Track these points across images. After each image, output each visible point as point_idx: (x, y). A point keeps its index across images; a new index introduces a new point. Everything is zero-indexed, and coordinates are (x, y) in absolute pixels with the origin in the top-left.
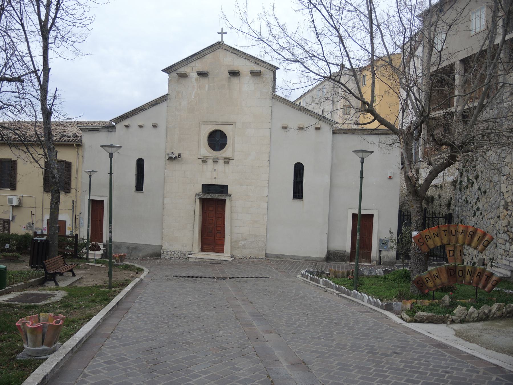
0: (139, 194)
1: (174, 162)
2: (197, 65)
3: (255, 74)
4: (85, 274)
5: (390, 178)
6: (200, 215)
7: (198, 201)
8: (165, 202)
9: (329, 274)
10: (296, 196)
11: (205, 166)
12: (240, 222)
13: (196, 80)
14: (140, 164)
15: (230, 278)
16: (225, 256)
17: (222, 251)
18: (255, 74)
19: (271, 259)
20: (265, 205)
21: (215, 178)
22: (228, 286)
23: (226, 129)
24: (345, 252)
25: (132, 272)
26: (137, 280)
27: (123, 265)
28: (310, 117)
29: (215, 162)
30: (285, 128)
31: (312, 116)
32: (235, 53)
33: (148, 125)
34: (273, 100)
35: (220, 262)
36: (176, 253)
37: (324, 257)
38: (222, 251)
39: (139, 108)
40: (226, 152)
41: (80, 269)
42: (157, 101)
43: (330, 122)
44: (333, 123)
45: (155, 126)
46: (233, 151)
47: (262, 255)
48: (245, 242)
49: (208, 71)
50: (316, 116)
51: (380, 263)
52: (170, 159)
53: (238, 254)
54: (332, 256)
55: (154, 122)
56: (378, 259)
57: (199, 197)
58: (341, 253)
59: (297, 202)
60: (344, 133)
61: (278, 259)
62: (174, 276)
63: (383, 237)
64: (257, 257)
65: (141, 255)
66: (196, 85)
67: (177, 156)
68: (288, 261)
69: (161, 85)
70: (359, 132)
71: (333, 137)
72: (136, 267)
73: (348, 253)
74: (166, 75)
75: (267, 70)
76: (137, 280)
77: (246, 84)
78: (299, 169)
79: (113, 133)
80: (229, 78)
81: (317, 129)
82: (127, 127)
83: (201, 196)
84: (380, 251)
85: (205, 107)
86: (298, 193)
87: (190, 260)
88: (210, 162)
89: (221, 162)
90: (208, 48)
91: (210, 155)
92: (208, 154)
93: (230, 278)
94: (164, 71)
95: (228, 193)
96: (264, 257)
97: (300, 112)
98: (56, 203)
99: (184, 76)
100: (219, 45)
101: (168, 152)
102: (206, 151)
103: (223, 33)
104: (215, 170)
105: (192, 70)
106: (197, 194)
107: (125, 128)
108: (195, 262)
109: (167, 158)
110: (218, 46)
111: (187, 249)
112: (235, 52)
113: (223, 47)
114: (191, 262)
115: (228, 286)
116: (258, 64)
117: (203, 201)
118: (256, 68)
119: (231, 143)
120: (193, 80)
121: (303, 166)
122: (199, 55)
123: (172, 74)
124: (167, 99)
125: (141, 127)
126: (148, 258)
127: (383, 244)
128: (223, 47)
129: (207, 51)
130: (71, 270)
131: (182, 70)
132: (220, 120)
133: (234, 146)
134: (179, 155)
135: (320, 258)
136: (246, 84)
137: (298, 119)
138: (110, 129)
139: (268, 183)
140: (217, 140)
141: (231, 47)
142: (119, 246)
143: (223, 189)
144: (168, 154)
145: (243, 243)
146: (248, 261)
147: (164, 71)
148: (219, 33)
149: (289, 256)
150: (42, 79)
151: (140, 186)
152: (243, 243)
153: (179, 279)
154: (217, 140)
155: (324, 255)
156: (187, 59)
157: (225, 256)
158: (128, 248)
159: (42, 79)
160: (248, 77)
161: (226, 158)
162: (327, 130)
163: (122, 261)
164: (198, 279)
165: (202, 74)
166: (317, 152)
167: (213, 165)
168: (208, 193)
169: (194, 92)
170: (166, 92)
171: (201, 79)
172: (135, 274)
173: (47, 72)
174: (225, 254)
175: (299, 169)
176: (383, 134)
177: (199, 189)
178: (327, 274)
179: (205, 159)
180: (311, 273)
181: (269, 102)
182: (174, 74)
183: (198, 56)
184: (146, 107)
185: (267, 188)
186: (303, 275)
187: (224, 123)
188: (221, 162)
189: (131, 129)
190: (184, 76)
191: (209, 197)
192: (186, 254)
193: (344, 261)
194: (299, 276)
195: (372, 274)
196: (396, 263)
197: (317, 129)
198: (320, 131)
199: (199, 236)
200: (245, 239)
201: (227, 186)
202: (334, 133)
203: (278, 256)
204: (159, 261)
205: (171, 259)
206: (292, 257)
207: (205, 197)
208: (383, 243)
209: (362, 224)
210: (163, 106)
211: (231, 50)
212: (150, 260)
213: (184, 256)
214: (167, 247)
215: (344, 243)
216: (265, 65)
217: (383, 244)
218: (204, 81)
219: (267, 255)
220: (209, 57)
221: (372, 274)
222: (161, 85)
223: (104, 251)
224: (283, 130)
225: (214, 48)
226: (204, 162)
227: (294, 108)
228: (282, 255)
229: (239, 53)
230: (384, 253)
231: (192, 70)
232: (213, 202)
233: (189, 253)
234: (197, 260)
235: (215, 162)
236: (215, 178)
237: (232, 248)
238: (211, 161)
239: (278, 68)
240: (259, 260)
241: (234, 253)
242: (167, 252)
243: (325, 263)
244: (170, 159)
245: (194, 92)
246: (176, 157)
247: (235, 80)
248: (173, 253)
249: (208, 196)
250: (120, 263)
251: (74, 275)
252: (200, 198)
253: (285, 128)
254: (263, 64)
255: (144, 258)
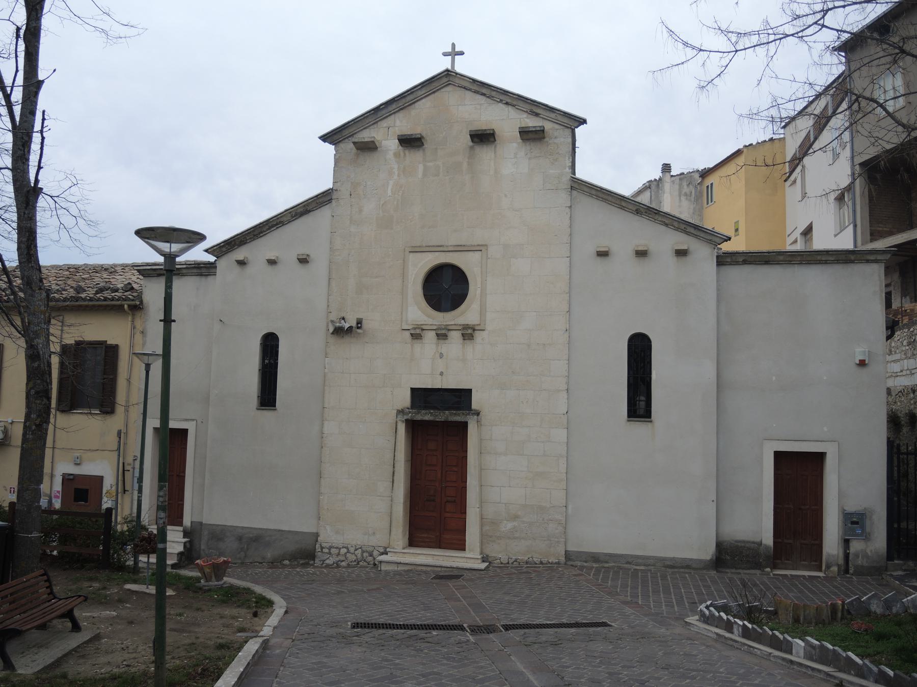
0: (267, 414)
1: (347, 339)
2: (398, 123)
3: (531, 136)
4: (112, 621)
5: (862, 363)
6: (406, 461)
7: (402, 428)
8: (326, 430)
9: (775, 613)
10: (635, 411)
11: (417, 346)
12: (502, 477)
13: (396, 155)
14: (270, 344)
15: (507, 628)
16: (468, 559)
17: (461, 546)
18: (531, 136)
19: (579, 564)
20: (560, 435)
21: (442, 374)
22: (520, 666)
23: (467, 262)
24: (760, 544)
25: (243, 611)
26: (252, 646)
27: (221, 587)
28: (663, 228)
29: (442, 336)
30: (603, 254)
31: (667, 225)
32: (483, 94)
33: (289, 257)
34: (574, 192)
35: (456, 573)
36: (352, 550)
37: (708, 557)
38: (461, 546)
39: (268, 221)
40: (468, 313)
41: (103, 602)
42: (308, 205)
43: (713, 238)
44: (718, 240)
45: (304, 261)
46: (483, 311)
47: (557, 554)
48: (516, 524)
49: (424, 134)
50: (676, 224)
51: (847, 571)
52: (339, 332)
53: (500, 552)
54: (729, 556)
55: (302, 251)
56: (841, 561)
57: (406, 417)
58: (749, 549)
59: (639, 428)
60: (745, 262)
61: (595, 565)
62: (356, 625)
63: (852, 506)
64: (545, 560)
65: (269, 555)
66: (396, 166)
67: (354, 324)
68: (620, 568)
69: (317, 169)
70: (781, 258)
71: (718, 273)
72: (253, 592)
73: (767, 547)
74: (330, 149)
75: (557, 126)
76: (252, 646)
77: (511, 160)
78: (640, 350)
79: (210, 278)
80: (472, 148)
81: (681, 253)
82: (241, 263)
83: (409, 417)
84: (846, 542)
85: (416, 210)
86: (639, 404)
87: (384, 567)
88: (430, 336)
89: (455, 336)
90: (423, 85)
91: (430, 321)
92: (426, 318)
93: (507, 628)
94: (325, 138)
95: (474, 406)
96: (563, 559)
97: (637, 218)
98: (39, 426)
99: (368, 147)
100: (447, 78)
101: (333, 317)
102: (418, 312)
103: (454, 53)
104: (441, 356)
105: (385, 137)
106: (401, 412)
107: (237, 269)
108: (397, 573)
109: (331, 329)
110: (445, 80)
111: (377, 541)
112: (484, 91)
113: (457, 81)
114: (387, 573)
115: (520, 666)
116: (537, 115)
117: (415, 429)
118: (532, 122)
119: (479, 292)
120: (390, 155)
121: (649, 341)
122: (404, 101)
123: (342, 145)
124: (330, 201)
125: (272, 262)
126: (287, 562)
127: (853, 523)
128: (457, 81)
129: (420, 93)
130: (69, 615)
131: (365, 136)
132: (453, 241)
133: (485, 300)
134: (359, 322)
135: (701, 561)
136: (511, 160)
137: (631, 232)
138: (204, 270)
139: (568, 383)
140: (446, 287)
141: (474, 81)
142: (219, 534)
143: (460, 398)
144: (332, 321)
145: (510, 525)
146: (527, 571)
147: (325, 138)
148: (445, 54)
149: (622, 556)
150: (17, 110)
151: (268, 397)
152: (510, 525)
153: (370, 636)
154: (446, 287)
155: (708, 553)
156: (377, 110)
157: (468, 559)
158: (240, 539)
159: (17, 110)
160: (515, 145)
161: (466, 327)
162: (704, 256)
163: (219, 578)
164: (422, 633)
165: (410, 142)
166: (678, 306)
167: (437, 344)
168: (425, 408)
169: (391, 183)
170: (328, 184)
171: (407, 152)
172: (249, 616)
173: (33, 89)
174: (467, 554)
175: (640, 350)
176: (837, 262)
177: (405, 399)
178: (767, 611)
179: (418, 331)
180: (725, 608)
181: (563, 198)
182: (348, 146)
183: (401, 103)
184: (285, 219)
185: (565, 395)
186: (706, 619)
187: (461, 249)
188: (455, 336)
189: (249, 270)
190: (368, 147)
191: (427, 418)
192: (375, 553)
193: (758, 566)
194: (693, 619)
195: (894, 610)
196: (886, 570)
197: (681, 253)
198: (688, 259)
199: (405, 509)
200: (516, 517)
201: (470, 391)
202: (723, 260)
203: (595, 558)
204: (311, 570)
205: (338, 566)
206: (630, 560)
207: (419, 417)
208: (854, 522)
209: (798, 475)
210: (323, 215)
211: (475, 87)
212: (293, 567)
213: (370, 559)
214: (329, 536)
215: (757, 523)
216: (553, 115)
217: (853, 523)
218: (414, 157)
219: (568, 555)
220: (425, 106)
221: (894, 610)
222: (317, 169)
223: (185, 546)
224: (599, 259)
225: (435, 84)
226: (416, 336)
227: (622, 208)
228: (606, 555)
229: (494, 94)
230: (856, 546)
231: (385, 137)
232: (438, 427)
233: (382, 550)
234: (401, 568)
235: (442, 336)
236: (442, 374)
237: (484, 538)
238: (433, 334)
239: (584, 122)
240: (551, 567)
241: (489, 551)
242: (330, 548)
243: (713, 573)
244: (339, 332)
245: (391, 183)
246: (351, 327)
247: (485, 153)
248: (345, 550)
249: (426, 416)
250: (214, 583)
251: (76, 627)
252: (407, 421)
253: (603, 254)
254: (548, 114)
255: (274, 563)
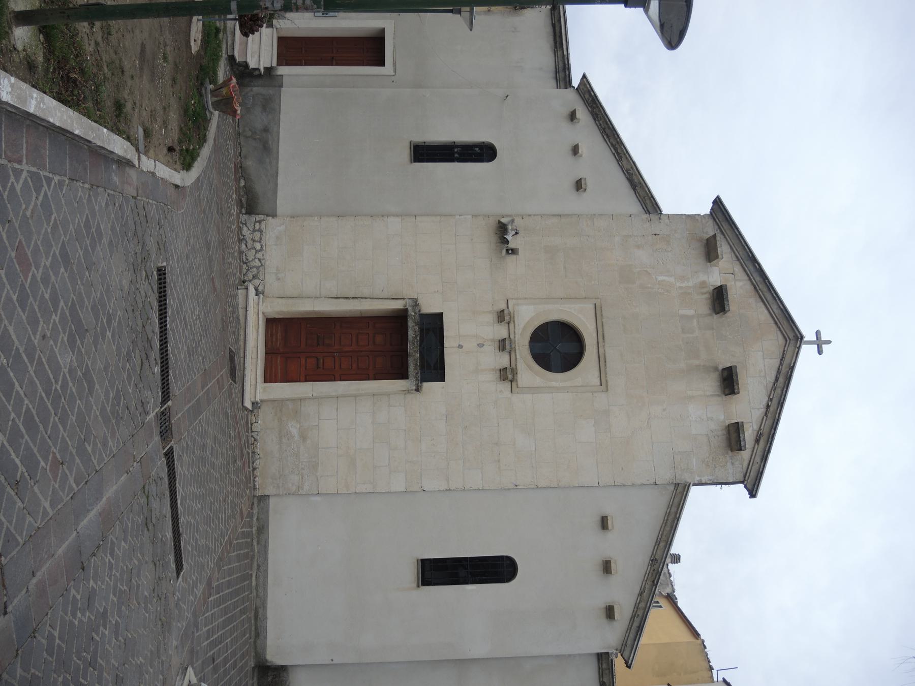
0: (405, 154)
1: (494, 239)
2: (739, 284)
3: (733, 436)
6: (361, 311)
7: (398, 305)
8: (391, 219)
11: (491, 318)
12: (347, 425)
13: (703, 284)
14: (483, 153)
15: (169, 455)
16: (255, 386)
17: (269, 378)
18: (734, 436)
19: (255, 511)
20: (399, 484)
21: (460, 347)
22: (110, 492)
25: (175, 135)
26: (118, 146)
27: (205, 109)
28: (637, 590)
29: (503, 345)
30: (604, 523)
31: (641, 594)
32: (777, 379)
33: (582, 169)
34: (672, 487)
35: (238, 374)
36: (259, 255)
37: (269, 657)
38: (269, 378)
39: (621, 143)
40: (530, 373)
42: (642, 187)
44: (626, 654)
45: (579, 185)
47: (265, 486)
48: (297, 438)
49: (728, 314)
50: (642, 605)
52: (502, 229)
53: (264, 422)
55: (590, 183)
57: (410, 309)
59: (411, 573)
61: (254, 529)
62: (162, 272)
64: (257, 473)
65: (250, 163)
66: (690, 284)
67: (511, 246)
68: (253, 557)
69: (682, 194)
71: (590, 654)
72: (201, 146)
75: (745, 464)
76: (118, 146)
77: (706, 414)
78: (498, 570)
79: (553, 83)
80: (716, 369)
81: (610, 612)
82: (572, 116)
83: (411, 312)
86: (438, 572)
87: (241, 292)
88: (502, 332)
89: (504, 360)
91: (519, 330)
92: (522, 326)
93: (169, 455)
94: (718, 203)
95: (425, 385)
99: (710, 252)
100: (792, 337)
101: (518, 222)
102: (529, 317)
103: (820, 344)
104: (481, 345)
106: (416, 303)
107: (566, 111)
108: (235, 308)
109: (504, 220)
110: (791, 335)
111: (271, 284)
112: (781, 380)
113: (791, 349)
114: (235, 297)
115: (110, 492)
116: (757, 441)
117: (398, 319)
118: (749, 435)
119: (554, 384)
122: (765, 289)
123: (711, 222)
124: (648, 212)
125: (575, 150)
126: (242, 183)
128: (791, 349)
129: (775, 307)
131: (723, 248)
132: (611, 352)
134: (514, 251)
135: (265, 649)
136: (706, 414)
138: (562, 74)
139: (457, 490)
140: (558, 346)
141: (792, 368)
142: (270, 106)
143: (434, 369)
144: (513, 221)
145: (295, 431)
146: (244, 455)
147: (718, 203)
149: (266, 559)
151: (425, 153)
152: (295, 431)
154: (558, 346)
155: (274, 657)
157: (255, 386)
158: (266, 130)
160: (722, 417)
161: (514, 372)
162: (607, 638)
163: (216, 105)
164: (155, 354)
165: (719, 299)
166: (549, 614)
167: (493, 340)
168: (421, 330)
169: (672, 280)
170: (666, 209)
171: (707, 296)
172: (168, 142)
174: (260, 385)
175: (498, 570)
177: (430, 307)
179: (507, 318)
181: (665, 475)
182: (710, 230)
183: (762, 286)
184: (624, 162)
188: (504, 360)
189: (565, 125)
190: (710, 252)
191: (411, 333)
192: (257, 282)
197: (610, 612)
198: (604, 620)
199: (307, 312)
200: (303, 437)
201: (443, 380)
202: (604, 661)
203: (263, 529)
204: (235, 210)
205: (240, 241)
206: (262, 568)
207: (410, 323)
210: (631, 204)
211: (784, 369)
212: (238, 188)
213: (250, 276)
214: (273, 228)
216: (758, 459)
218: (703, 304)
219: (264, 498)
220: (760, 314)
222: (682, 194)
223: (255, 69)
224: (599, 519)
225: (785, 324)
226: (501, 316)
227: (658, 543)
228: (267, 541)
229: (779, 391)
232: (398, 346)
233: (260, 289)
234: (241, 312)
235: (503, 345)
236: (460, 347)
237: (279, 403)
238: (505, 335)
239: (753, 494)
240: (250, 482)
241: (264, 408)
242: (260, 231)
244: (502, 229)
245: (672, 280)
246: (507, 242)
247: (711, 384)
248: (258, 248)
249: (412, 332)
250: (210, 100)
252: (406, 310)
253: (604, 523)
255: (241, 170)
